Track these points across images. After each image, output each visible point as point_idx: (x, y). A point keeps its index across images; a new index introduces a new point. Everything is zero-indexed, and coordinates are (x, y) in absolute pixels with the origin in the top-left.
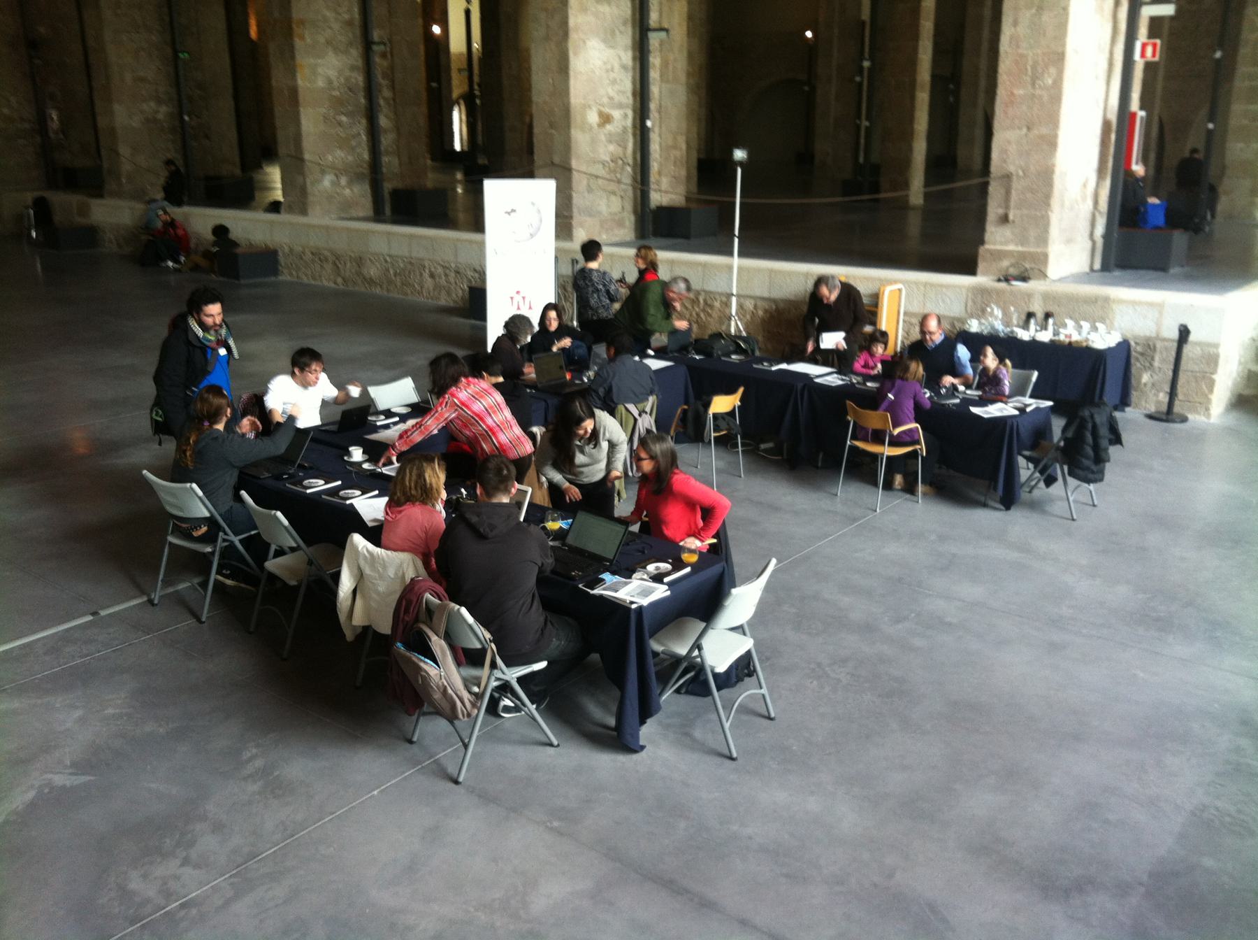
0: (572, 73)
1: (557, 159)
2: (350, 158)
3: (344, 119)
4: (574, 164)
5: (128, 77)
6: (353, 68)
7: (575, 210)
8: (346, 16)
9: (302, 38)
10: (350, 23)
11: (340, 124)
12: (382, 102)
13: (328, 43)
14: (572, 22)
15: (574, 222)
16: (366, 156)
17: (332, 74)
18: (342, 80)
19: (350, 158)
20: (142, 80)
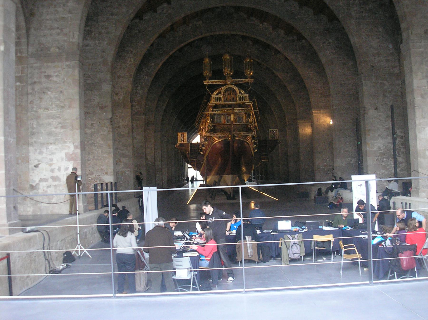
0: (418, 139)
1: (415, 169)
2: (386, 172)
3: (385, 159)
4: (420, 170)
5: (342, 151)
6: (389, 143)
7: (421, 186)
8: (387, 127)
9: (370, 135)
10: (388, 129)
11: (383, 161)
12: (400, 153)
13: (379, 136)
14: (417, 122)
15: (420, 191)
16: (393, 171)
17: (380, 145)
18: (384, 147)
19: (386, 172)
20: (347, 151)
